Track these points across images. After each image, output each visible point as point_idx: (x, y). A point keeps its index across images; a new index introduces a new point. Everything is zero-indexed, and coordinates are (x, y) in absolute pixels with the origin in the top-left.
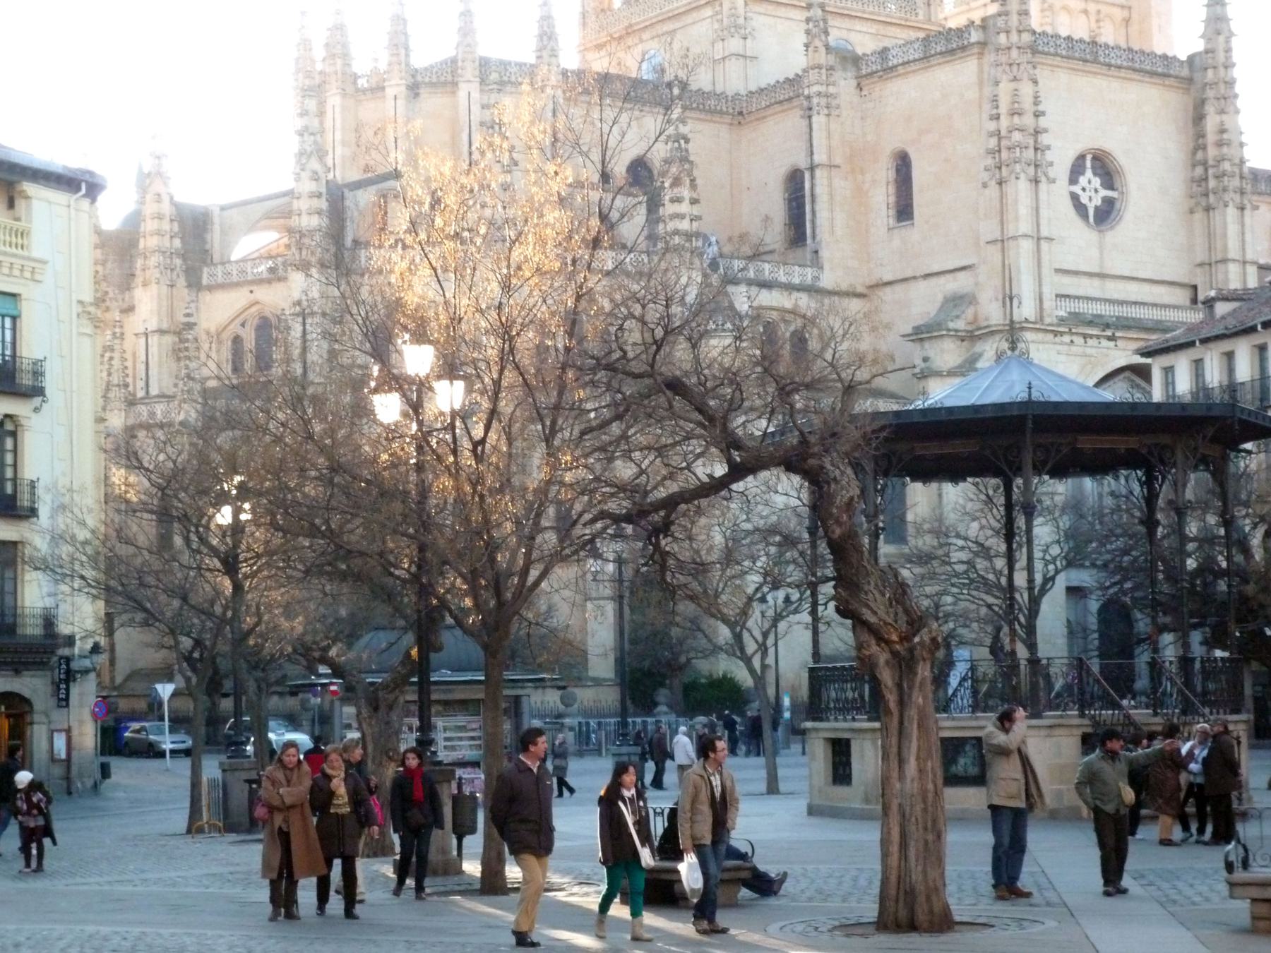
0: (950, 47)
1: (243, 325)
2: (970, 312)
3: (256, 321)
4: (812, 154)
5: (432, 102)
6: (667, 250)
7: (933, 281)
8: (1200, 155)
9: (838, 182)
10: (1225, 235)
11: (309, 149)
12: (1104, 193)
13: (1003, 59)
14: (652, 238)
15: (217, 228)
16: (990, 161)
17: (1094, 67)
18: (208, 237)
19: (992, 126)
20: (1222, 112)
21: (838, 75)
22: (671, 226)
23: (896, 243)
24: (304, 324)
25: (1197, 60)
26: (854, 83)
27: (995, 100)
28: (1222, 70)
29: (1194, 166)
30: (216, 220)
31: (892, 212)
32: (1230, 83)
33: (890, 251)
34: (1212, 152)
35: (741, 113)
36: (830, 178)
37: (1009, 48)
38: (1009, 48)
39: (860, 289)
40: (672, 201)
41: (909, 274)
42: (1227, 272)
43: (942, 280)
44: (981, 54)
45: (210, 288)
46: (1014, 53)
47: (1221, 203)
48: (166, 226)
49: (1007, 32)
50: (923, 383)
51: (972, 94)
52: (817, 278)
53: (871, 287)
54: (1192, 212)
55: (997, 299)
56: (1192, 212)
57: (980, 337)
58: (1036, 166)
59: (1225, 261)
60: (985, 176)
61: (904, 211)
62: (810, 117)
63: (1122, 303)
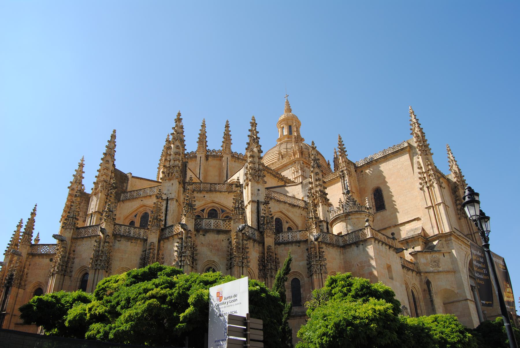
0: (395, 150)
1: (136, 216)
3: (141, 214)
5: (212, 162)
8: (458, 202)
15: (129, 182)
16: (420, 181)
18: (125, 185)
19: (419, 171)
24: (167, 203)
29: (457, 205)
30: (130, 179)
40: (316, 180)
41: (386, 226)
45: (123, 201)
48: (110, 174)
54: (460, 219)
56: (460, 219)
62: (343, 177)
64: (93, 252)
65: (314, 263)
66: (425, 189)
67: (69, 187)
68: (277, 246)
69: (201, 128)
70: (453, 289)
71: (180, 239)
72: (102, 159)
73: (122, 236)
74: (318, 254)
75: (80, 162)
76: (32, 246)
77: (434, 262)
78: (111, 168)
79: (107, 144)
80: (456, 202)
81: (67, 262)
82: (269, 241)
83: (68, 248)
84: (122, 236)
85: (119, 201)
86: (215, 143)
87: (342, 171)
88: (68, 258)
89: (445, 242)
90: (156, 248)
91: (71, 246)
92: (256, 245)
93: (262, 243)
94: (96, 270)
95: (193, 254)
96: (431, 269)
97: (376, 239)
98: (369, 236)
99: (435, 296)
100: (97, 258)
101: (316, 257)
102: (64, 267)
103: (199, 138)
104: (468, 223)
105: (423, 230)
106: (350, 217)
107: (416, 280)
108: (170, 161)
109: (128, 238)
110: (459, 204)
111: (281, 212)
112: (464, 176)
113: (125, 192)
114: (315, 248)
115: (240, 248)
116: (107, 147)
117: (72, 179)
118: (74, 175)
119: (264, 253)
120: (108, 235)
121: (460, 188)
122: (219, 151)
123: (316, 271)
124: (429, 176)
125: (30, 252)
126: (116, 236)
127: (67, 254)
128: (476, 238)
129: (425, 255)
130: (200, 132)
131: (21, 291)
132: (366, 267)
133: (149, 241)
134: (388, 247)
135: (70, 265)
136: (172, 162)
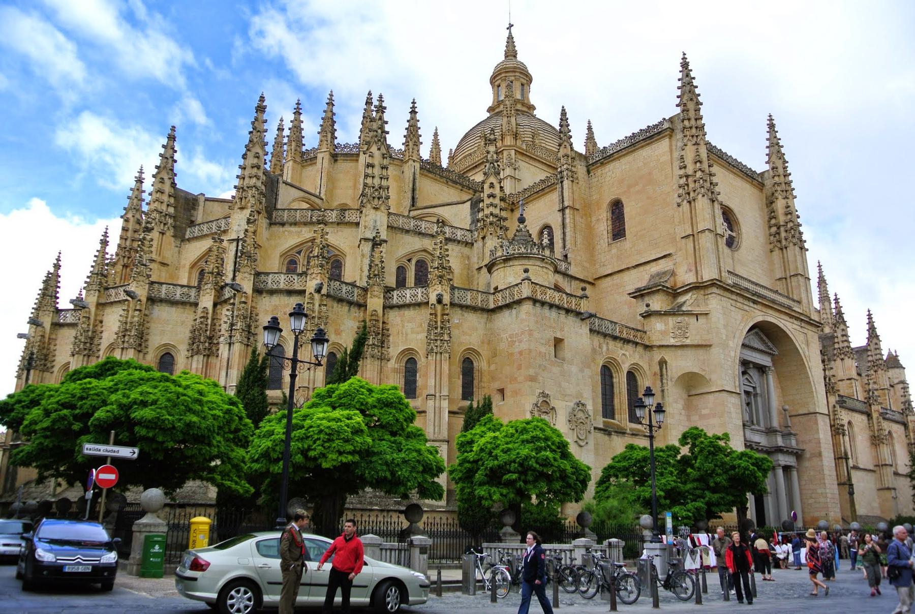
2: (672, 279)
4: (563, 201)
6: (485, 226)
7: (641, 269)
8: (773, 221)
9: (578, 218)
10: (796, 261)
11: (255, 140)
12: (730, 232)
13: (688, 133)
14: (475, 221)
15: (201, 208)
16: (681, 191)
17: (723, 163)
19: (682, 172)
20: (786, 198)
21: (577, 162)
22: (487, 211)
23: (614, 251)
24: (238, 246)
25: (766, 175)
26: (585, 169)
27: (682, 158)
28: (782, 177)
30: (201, 203)
31: (610, 235)
32: (789, 183)
33: (609, 256)
34: (782, 219)
35: (513, 203)
36: (574, 215)
37: (691, 128)
38: (691, 128)
39: (590, 280)
40: (489, 196)
42: (798, 281)
43: (647, 267)
44: (671, 136)
45: (189, 240)
46: (694, 130)
47: (791, 244)
48: (165, 198)
49: (689, 119)
50: (648, 320)
51: (667, 157)
52: (567, 269)
53: (596, 279)
54: (771, 252)
55: (691, 271)
57: (680, 294)
58: (712, 193)
59: (797, 275)
60: (679, 200)
61: (618, 232)
62: (562, 182)
63: (757, 284)
64: (118, 324)
65: (432, 337)
66: (685, 204)
67: (122, 217)
68: (388, 310)
69: (325, 107)
70: (703, 373)
71: (231, 304)
72: (154, 176)
73: (161, 301)
74: (439, 323)
75: (137, 175)
76: (58, 311)
77: (679, 329)
78: (167, 188)
79: (162, 151)
80: (769, 221)
81: (92, 338)
82: (375, 303)
83: (92, 318)
84: (161, 301)
85: (183, 240)
86: (349, 133)
87: (561, 172)
88: (94, 332)
89: (702, 297)
90: (210, 316)
91: (96, 315)
92: (354, 310)
93: (362, 306)
94: (123, 349)
95: (249, 326)
96: (672, 342)
97: (535, 301)
98: (524, 296)
99: (669, 383)
100: (124, 333)
101: (436, 328)
102: (88, 345)
103: (321, 126)
104: (783, 258)
105: (673, 274)
106: (511, 263)
107: (641, 357)
108: (244, 178)
109: (173, 303)
110: (775, 225)
111: (425, 251)
112: (790, 174)
113: (192, 223)
114: (436, 315)
115: (313, 317)
116: (161, 155)
117: (126, 203)
118: (129, 198)
119: (364, 321)
120: (140, 300)
121: (780, 197)
122: (356, 146)
123: (432, 349)
124: (695, 181)
125: (55, 320)
126: (152, 300)
127: (91, 327)
128: (793, 284)
129: (664, 318)
130: (324, 115)
131: (47, 375)
132: (517, 344)
133: (201, 305)
134: (563, 312)
135: (96, 342)
136: (247, 180)
